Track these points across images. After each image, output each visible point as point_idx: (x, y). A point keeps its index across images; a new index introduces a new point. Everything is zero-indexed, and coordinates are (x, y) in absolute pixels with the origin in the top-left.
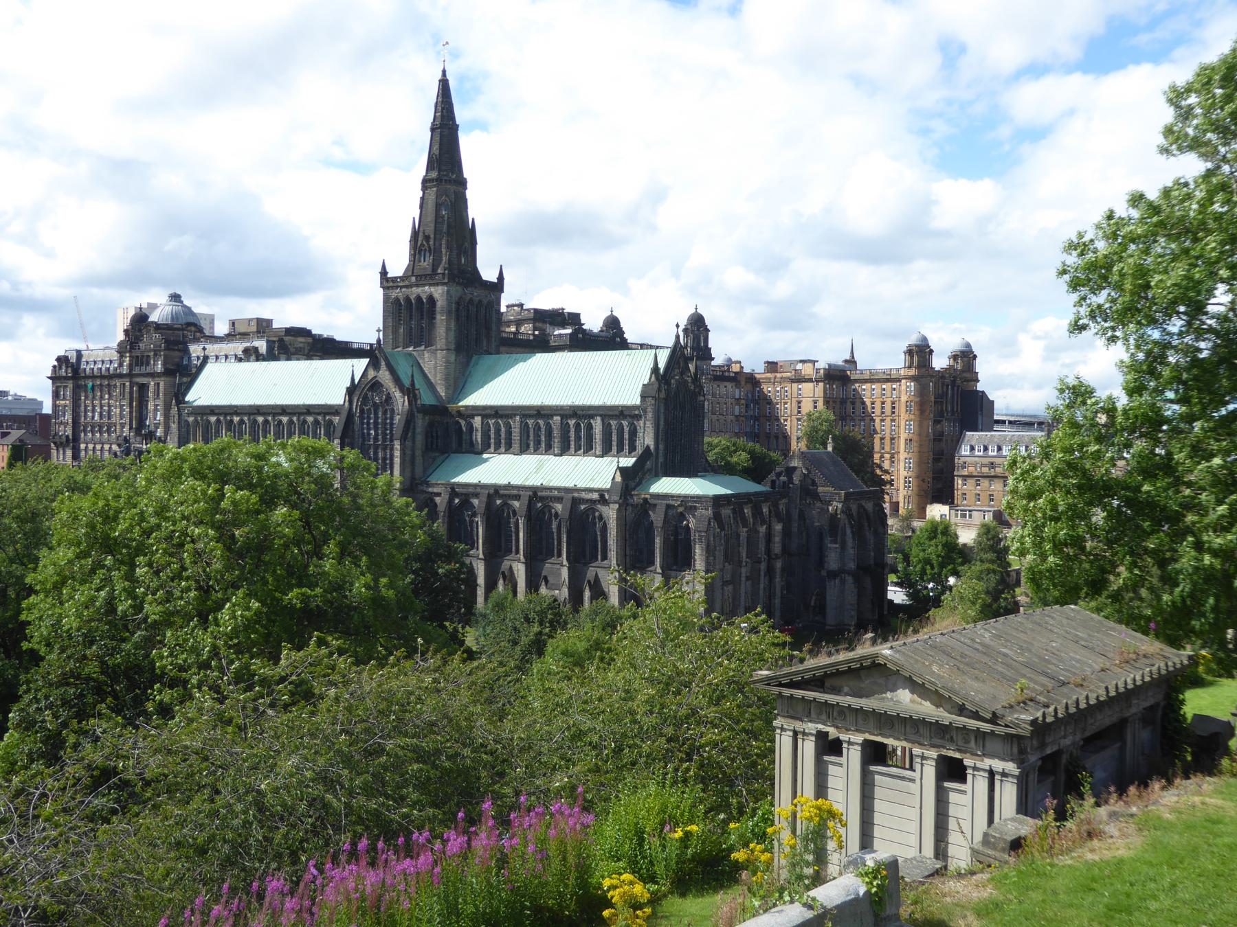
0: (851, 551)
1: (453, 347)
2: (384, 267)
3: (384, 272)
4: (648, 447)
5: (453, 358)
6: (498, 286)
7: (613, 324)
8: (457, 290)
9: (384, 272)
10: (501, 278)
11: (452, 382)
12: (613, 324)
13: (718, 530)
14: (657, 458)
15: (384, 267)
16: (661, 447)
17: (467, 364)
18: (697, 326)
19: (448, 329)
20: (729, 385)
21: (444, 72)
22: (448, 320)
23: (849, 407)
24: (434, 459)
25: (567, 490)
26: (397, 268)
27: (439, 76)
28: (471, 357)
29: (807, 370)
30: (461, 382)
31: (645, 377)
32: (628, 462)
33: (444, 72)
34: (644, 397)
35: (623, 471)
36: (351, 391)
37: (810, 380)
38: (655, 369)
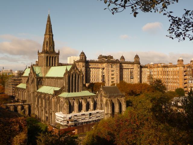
0: (110, 109)
1: (46, 65)
2: (38, 51)
3: (38, 52)
4: (64, 86)
5: (46, 68)
6: (58, 54)
7: (123, 58)
8: (46, 55)
9: (38, 52)
10: (59, 52)
11: (45, 71)
12: (123, 58)
13: (66, 105)
14: (66, 88)
15: (38, 51)
16: (67, 86)
17: (50, 68)
18: (137, 57)
19: (45, 62)
20: (146, 69)
21: (49, 15)
22: (45, 60)
23: (169, 72)
24: (41, 87)
25: (49, 94)
26: (41, 51)
27: (48, 16)
28: (50, 66)
29: (159, 65)
30: (46, 72)
31: (64, 72)
32: (58, 89)
33: (49, 15)
34: (64, 75)
35: (55, 91)
36: (29, 74)
37: (160, 67)
38: (67, 70)
